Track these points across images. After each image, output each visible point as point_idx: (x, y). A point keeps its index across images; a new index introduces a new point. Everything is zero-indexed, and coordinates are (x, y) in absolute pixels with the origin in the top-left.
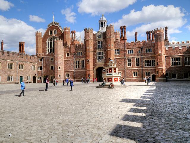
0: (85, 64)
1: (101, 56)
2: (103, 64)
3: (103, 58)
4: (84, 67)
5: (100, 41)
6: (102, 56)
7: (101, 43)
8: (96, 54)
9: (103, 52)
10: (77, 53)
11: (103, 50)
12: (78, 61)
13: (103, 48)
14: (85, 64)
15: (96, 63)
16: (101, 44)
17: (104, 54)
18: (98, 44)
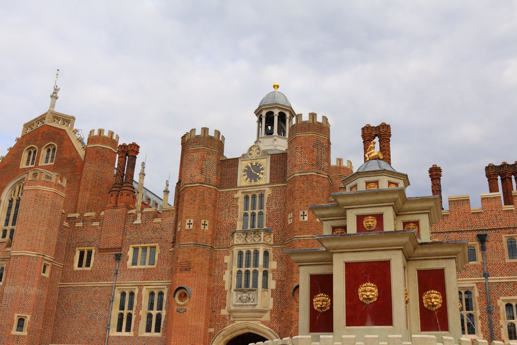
0: (164, 313)
1: (256, 272)
2: (267, 317)
3: (265, 286)
4: (157, 330)
5: (254, 196)
6: (260, 270)
7: (261, 207)
8: (227, 259)
9: (266, 253)
10: (130, 253)
11: (270, 240)
12: (132, 294)
13: (267, 231)
14: (164, 313)
15: (224, 312)
16: (257, 211)
17: (273, 265)
18: (246, 208)
